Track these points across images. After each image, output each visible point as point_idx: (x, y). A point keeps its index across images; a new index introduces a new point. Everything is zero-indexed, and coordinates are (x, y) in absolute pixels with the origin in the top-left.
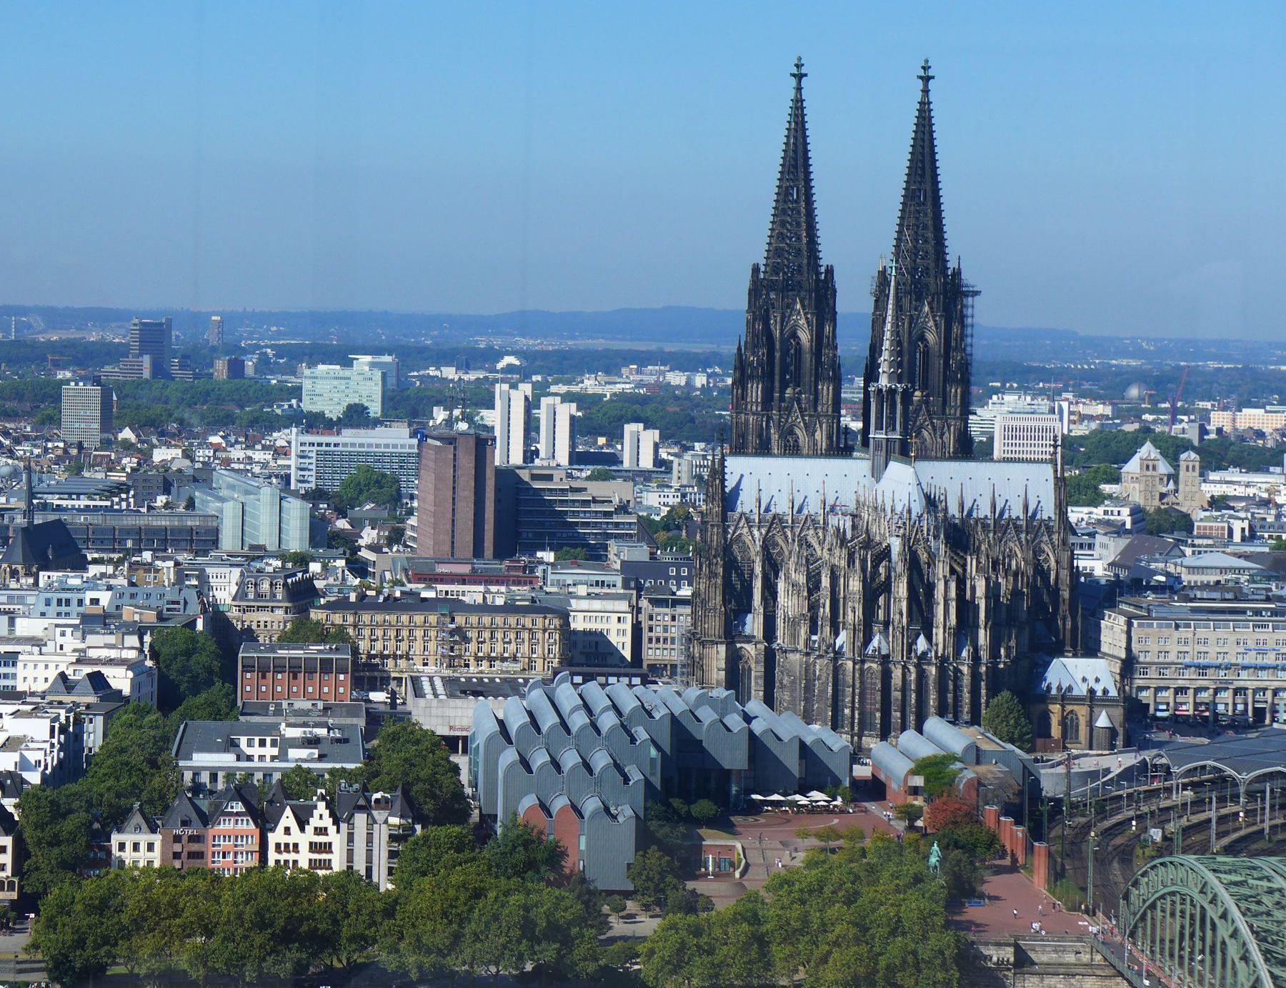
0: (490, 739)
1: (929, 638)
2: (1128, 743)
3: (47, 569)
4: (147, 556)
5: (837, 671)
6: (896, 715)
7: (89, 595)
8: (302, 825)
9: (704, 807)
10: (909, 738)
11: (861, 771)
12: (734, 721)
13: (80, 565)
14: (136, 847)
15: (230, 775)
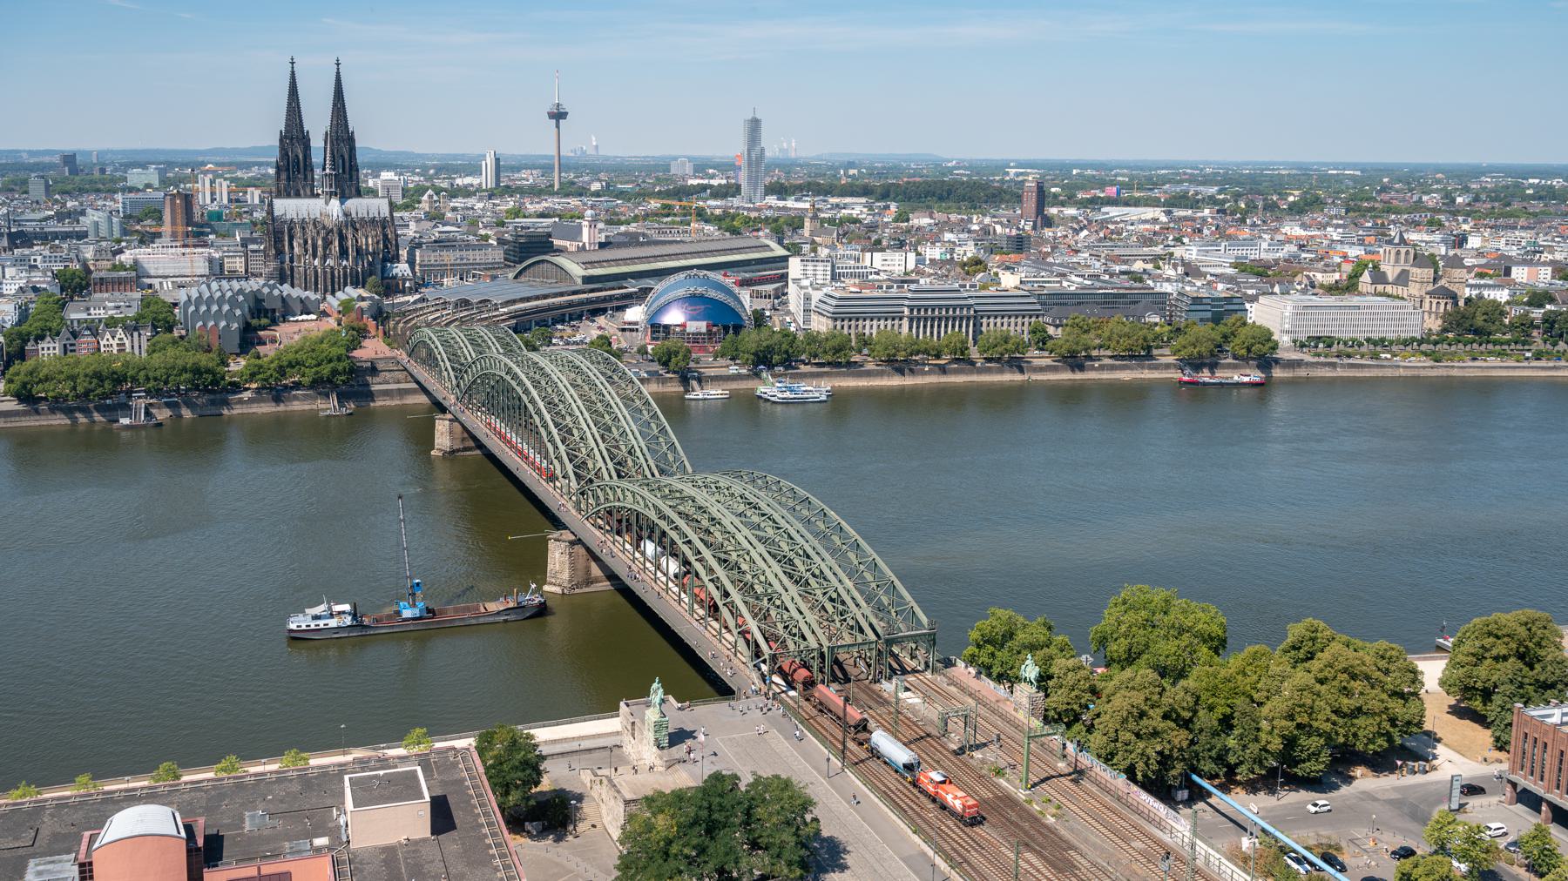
0: (185, 303)
1: (347, 260)
2: (417, 291)
3: (17, 248)
4: (57, 242)
5: (316, 272)
6: (336, 286)
7: (33, 257)
8: (113, 337)
9: (264, 321)
10: (339, 294)
11: (322, 307)
12: (276, 292)
13: (32, 246)
14: (49, 349)
15: (86, 320)
